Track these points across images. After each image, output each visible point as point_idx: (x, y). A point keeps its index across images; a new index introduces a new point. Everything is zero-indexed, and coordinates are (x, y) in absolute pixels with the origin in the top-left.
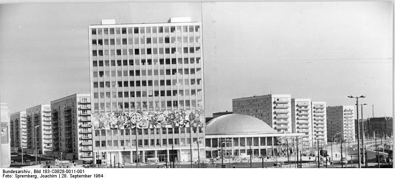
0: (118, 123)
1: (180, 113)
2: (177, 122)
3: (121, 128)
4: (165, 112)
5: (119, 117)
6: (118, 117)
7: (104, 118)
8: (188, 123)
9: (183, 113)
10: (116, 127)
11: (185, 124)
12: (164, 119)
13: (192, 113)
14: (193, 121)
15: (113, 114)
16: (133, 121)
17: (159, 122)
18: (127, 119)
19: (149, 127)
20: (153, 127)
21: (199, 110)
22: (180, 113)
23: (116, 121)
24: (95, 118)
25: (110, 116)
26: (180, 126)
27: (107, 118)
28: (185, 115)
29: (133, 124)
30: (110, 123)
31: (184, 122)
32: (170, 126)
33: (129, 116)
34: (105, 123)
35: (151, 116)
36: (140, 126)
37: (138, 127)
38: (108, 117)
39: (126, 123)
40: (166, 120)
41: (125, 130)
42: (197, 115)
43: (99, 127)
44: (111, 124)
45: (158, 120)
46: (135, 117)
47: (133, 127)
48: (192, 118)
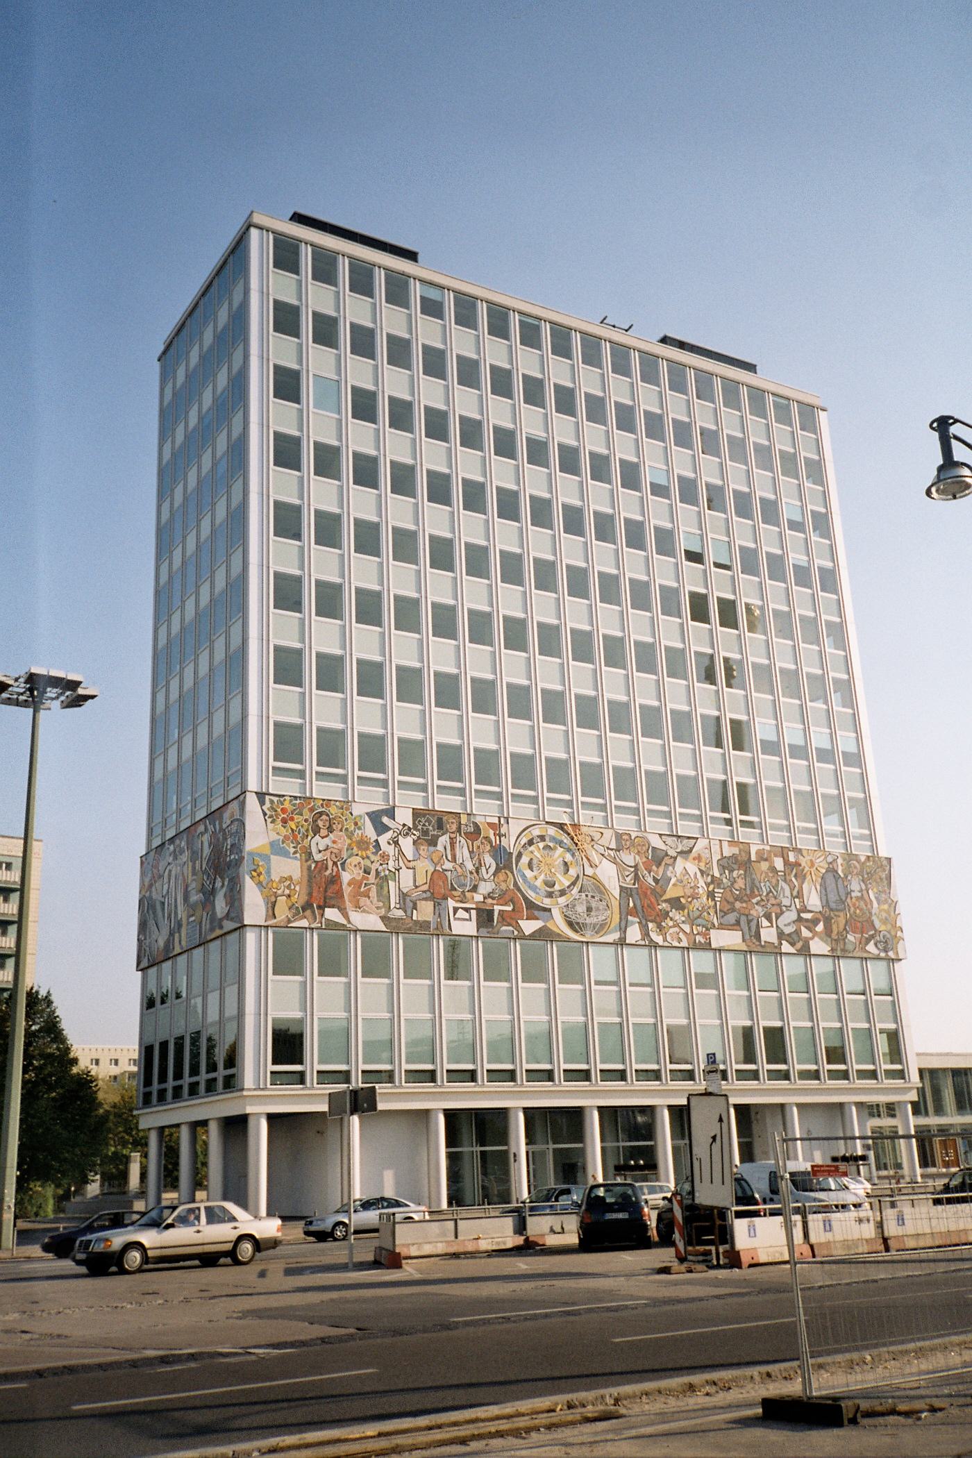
1: (779, 864)
2: (769, 918)
5: (444, 840)
6: (433, 842)
7: (338, 840)
8: (820, 928)
9: (786, 863)
10: (425, 911)
11: (805, 933)
12: (702, 890)
13: (832, 870)
14: (842, 921)
16: (531, 881)
17: (676, 903)
18: (489, 860)
19: (624, 931)
20: (646, 934)
21: (863, 859)
22: (779, 864)
23: (425, 866)
24: (276, 832)
25: (381, 829)
26: (786, 947)
27: (363, 844)
28: (801, 876)
29: (531, 905)
30: (382, 880)
31: (800, 919)
33: (510, 843)
34: (346, 877)
35: (629, 858)
36: (571, 924)
37: (559, 923)
38: (370, 831)
39: (485, 888)
40: (711, 895)
42: (855, 886)
43: (307, 906)
45: (671, 893)
46: (537, 851)
47: (529, 927)
48: (833, 897)
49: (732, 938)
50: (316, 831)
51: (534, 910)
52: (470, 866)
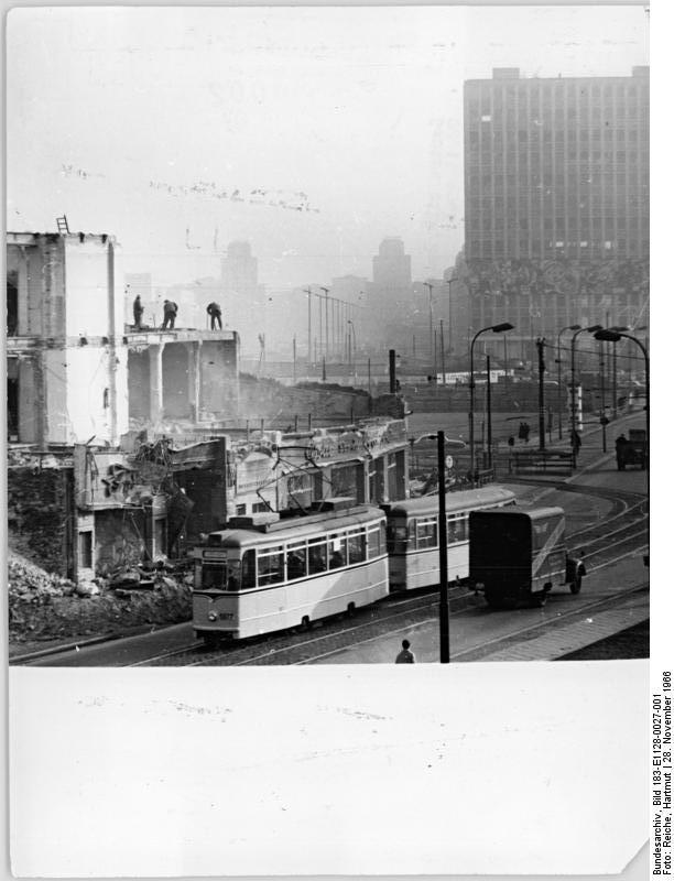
0: (519, 283)
3: (524, 293)
4: (611, 262)
10: (514, 289)
15: (509, 263)
18: (535, 274)
25: (501, 267)
32: (622, 290)
33: (542, 267)
37: (558, 290)
38: (498, 270)
41: (531, 298)
43: (479, 291)
44: (504, 284)
47: (547, 291)
49: (622, 290)
50: (482, 270)
51: (549, 286)
52: (528, 275)
